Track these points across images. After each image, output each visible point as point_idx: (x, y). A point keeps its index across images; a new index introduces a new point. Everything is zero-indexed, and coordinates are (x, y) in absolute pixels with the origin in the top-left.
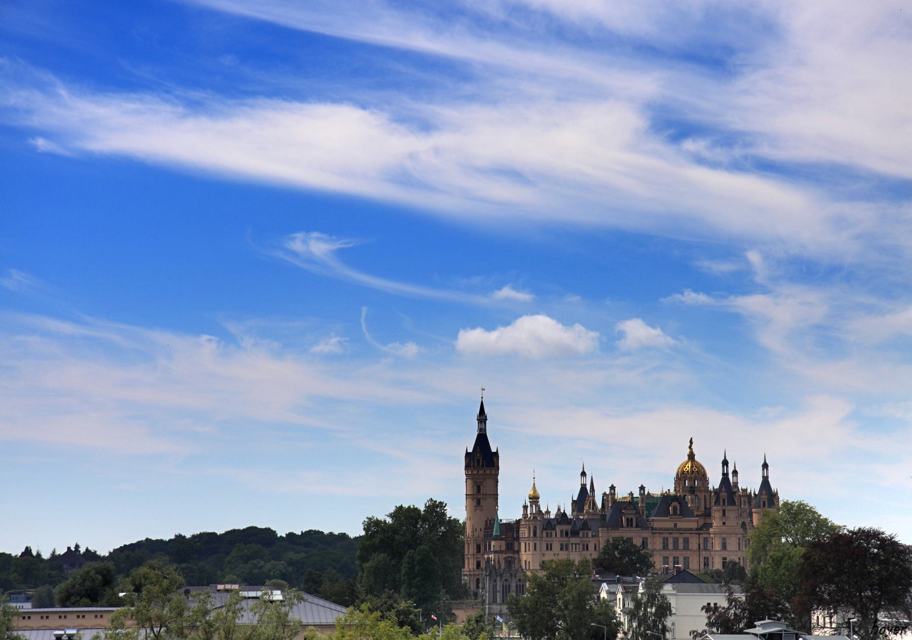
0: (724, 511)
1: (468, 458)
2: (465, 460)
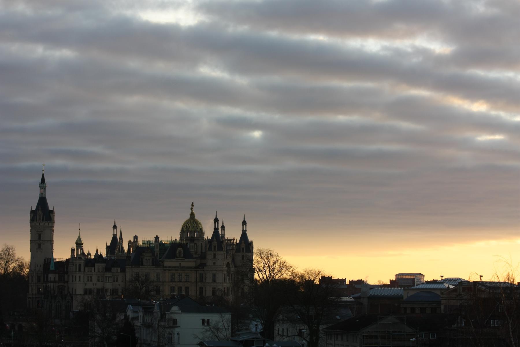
0: (215, 255)
1: (33, 214)
2: (30, 215)
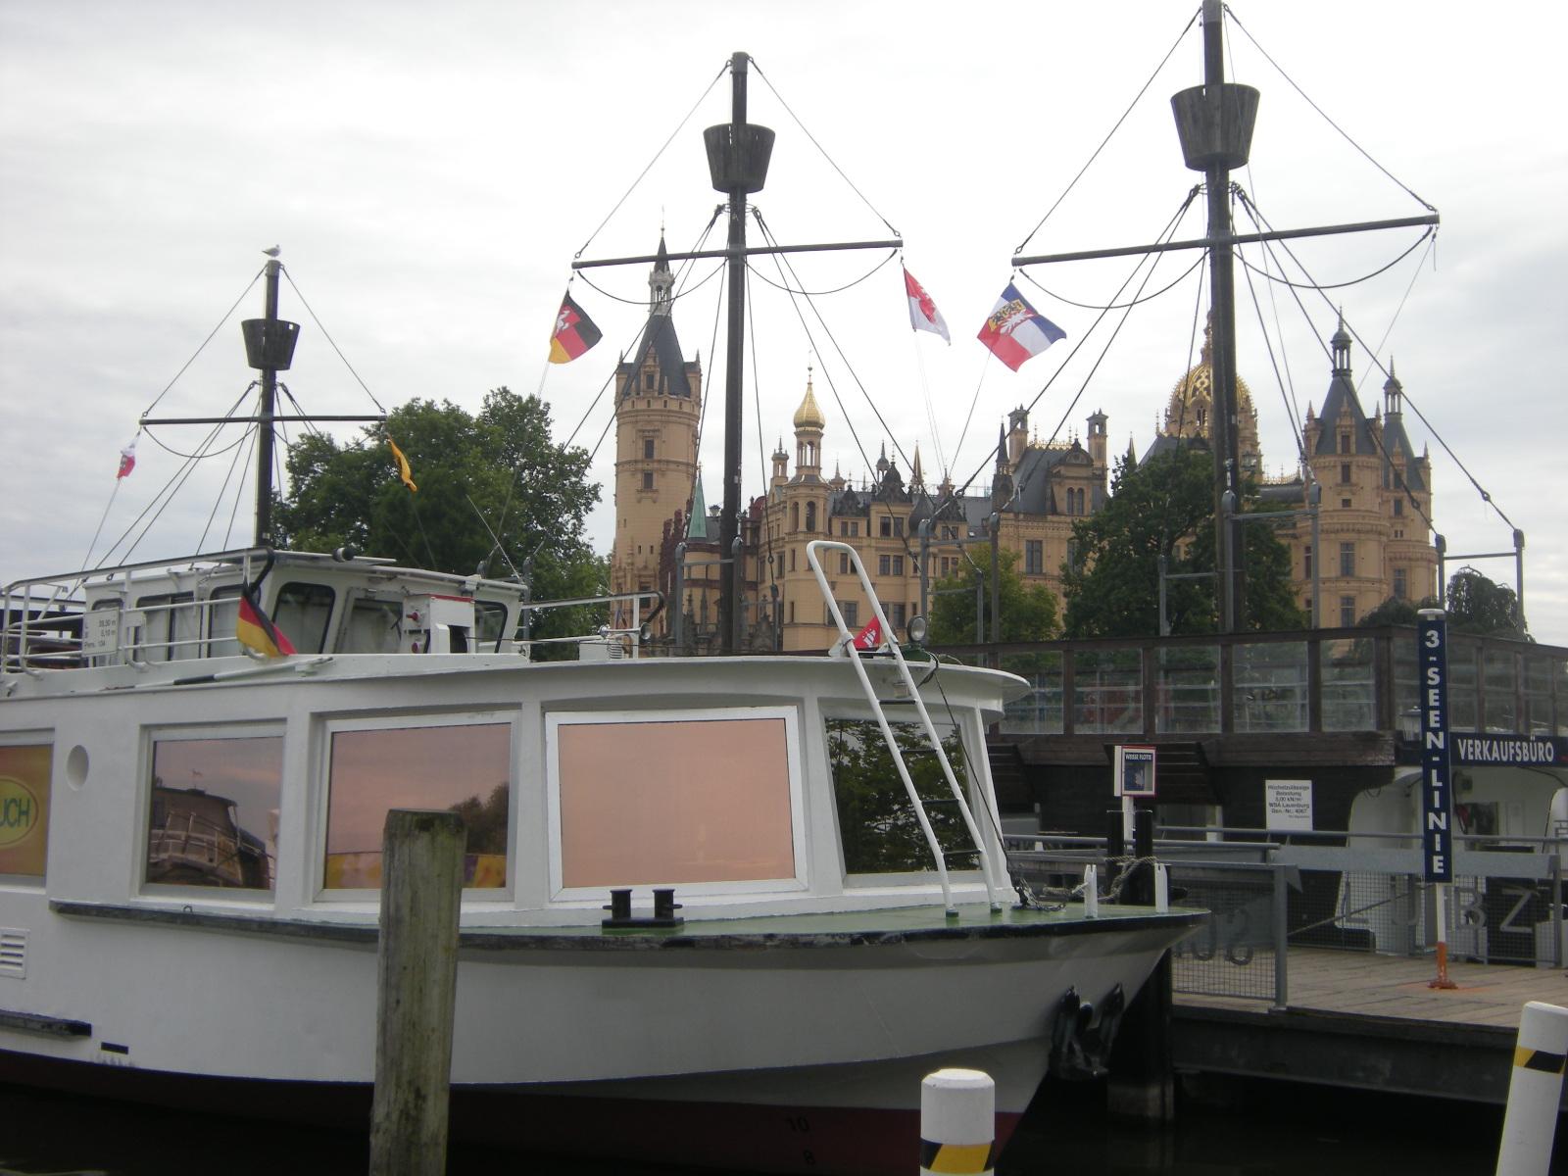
0: (1346, 469)
